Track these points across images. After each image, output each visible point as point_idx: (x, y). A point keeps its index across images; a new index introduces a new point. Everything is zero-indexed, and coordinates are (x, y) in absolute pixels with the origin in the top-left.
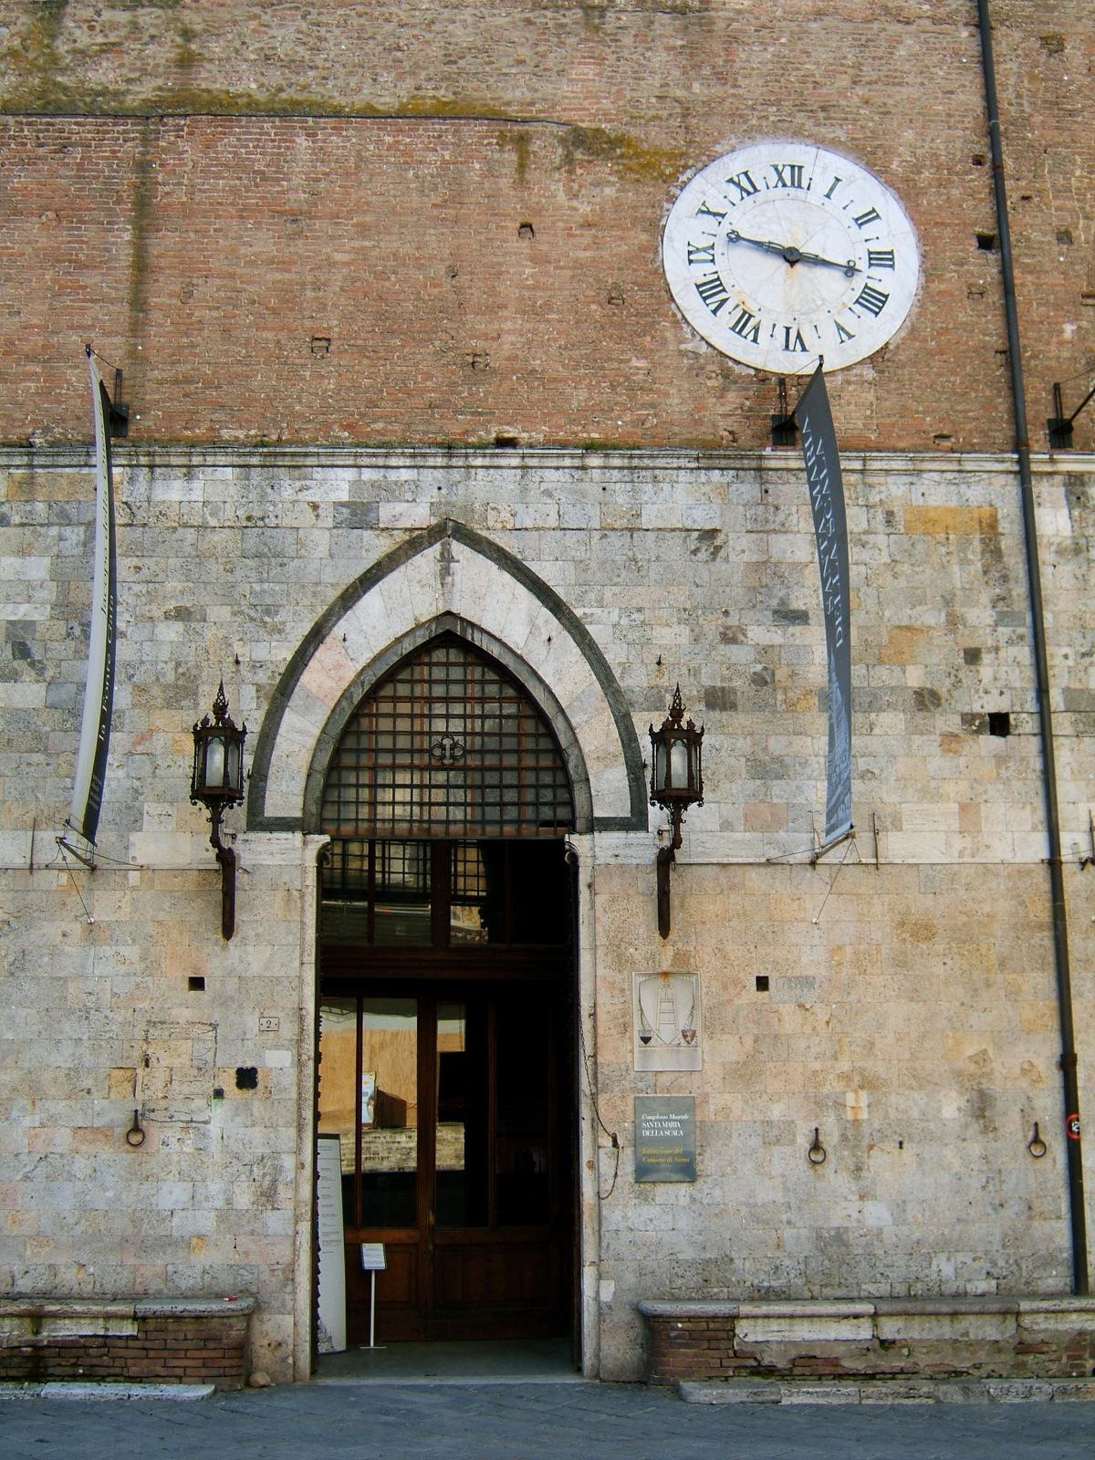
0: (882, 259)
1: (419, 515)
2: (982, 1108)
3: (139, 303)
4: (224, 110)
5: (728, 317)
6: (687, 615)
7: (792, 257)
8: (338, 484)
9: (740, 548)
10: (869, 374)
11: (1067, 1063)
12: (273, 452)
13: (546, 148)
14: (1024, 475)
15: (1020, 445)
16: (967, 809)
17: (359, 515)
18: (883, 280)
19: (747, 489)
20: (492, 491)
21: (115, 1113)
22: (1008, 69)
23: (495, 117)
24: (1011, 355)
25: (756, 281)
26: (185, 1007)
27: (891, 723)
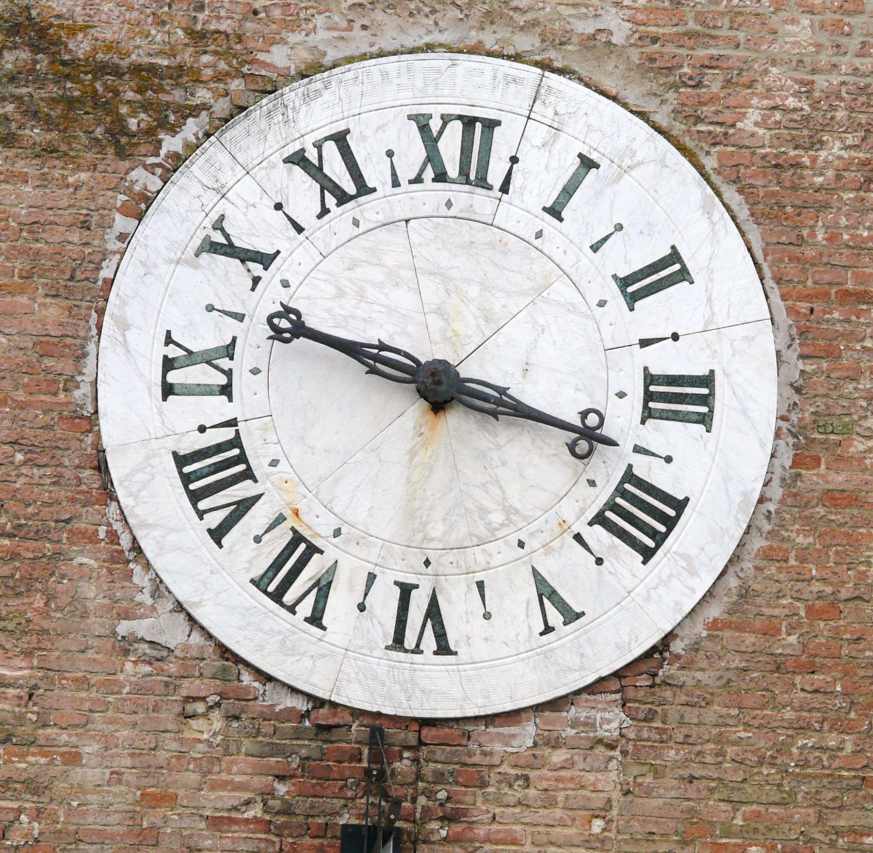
0: (680, 397)
5: (251, 549)
7: (439, 389)
10: (610, 720)
25: (337, 458)
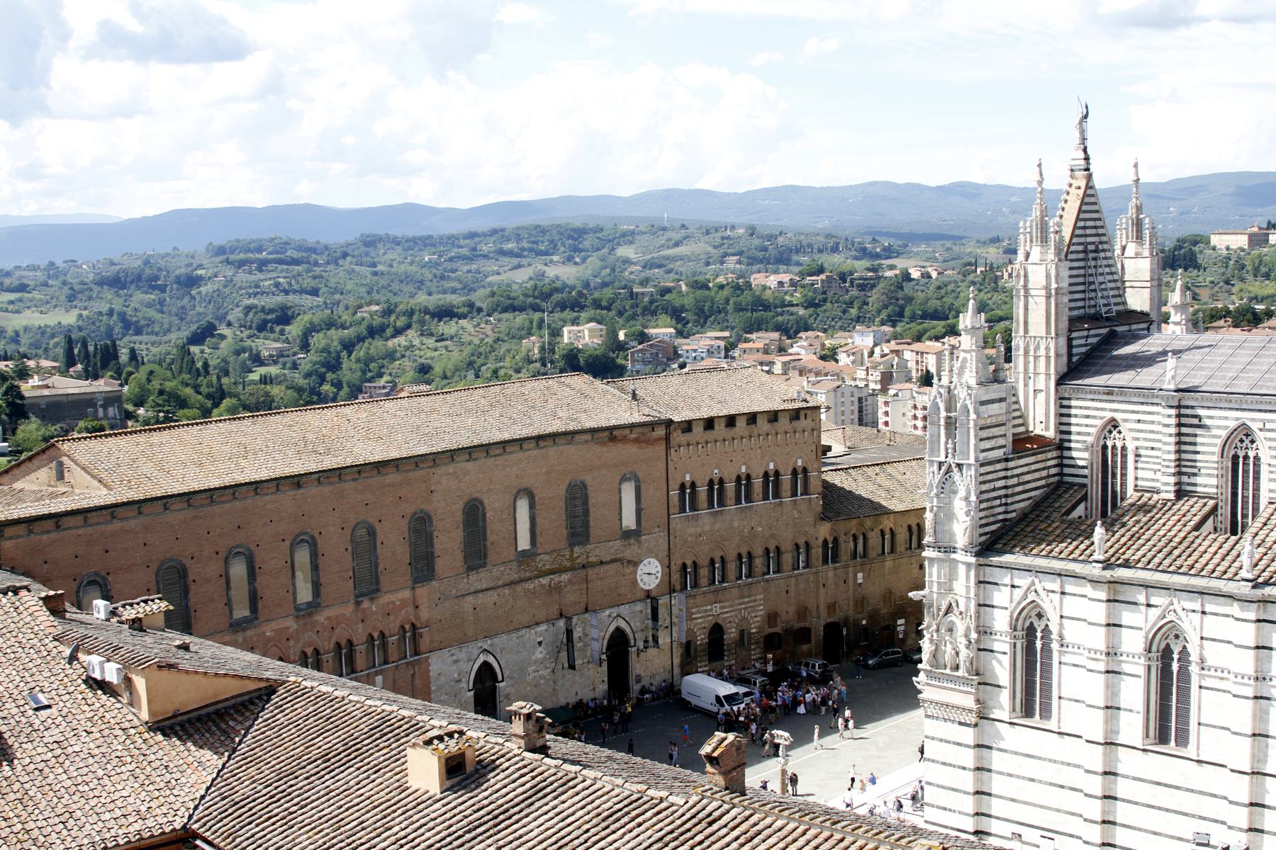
4: (593, 565)
8: (607, 613)
20: (624, 610)
25: (646, 578)
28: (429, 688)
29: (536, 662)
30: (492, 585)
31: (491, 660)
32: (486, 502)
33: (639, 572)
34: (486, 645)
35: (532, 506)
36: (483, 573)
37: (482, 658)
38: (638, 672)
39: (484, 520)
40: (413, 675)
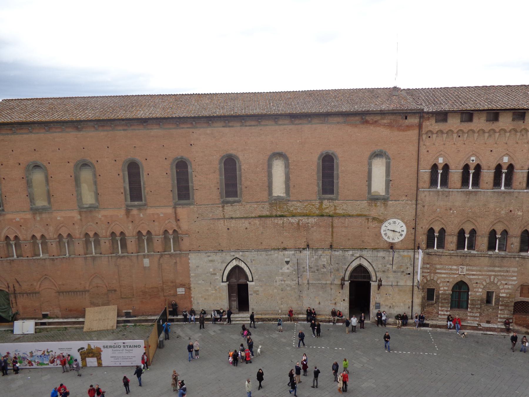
0: (403, 231)
1: (358, 255)
2: (404, 305)
3: (332, 235)
6: (382, 264)
7: (394, 231)
8: (351, 253)
9: (387, 258)
11: (412, 302)
12: (345, 250)
13: (370, 220)
14: (414, 252)
15: (414, 249)
16: (406, 282)
17: (352, 255)
18: (403, 233)
19: (388, 253)
20: (365, 253)
21: (334, 302)
22: (418, 209)
23: (365, 216)
24: (415, 240)
25: (390, 234)
26: (339, 295)
27: (399, 274)
28: (189, 274)
29: (282, 274)
30: (245, 216)
31: (242, 265)
32: (241, 158)
33: (383, 228)
34: (239, 255)
35: (287, 166)
36: (237, 206)
37: (234, 263)
38: (378, 300)
39: (240, 170)
40: (176, 263)
